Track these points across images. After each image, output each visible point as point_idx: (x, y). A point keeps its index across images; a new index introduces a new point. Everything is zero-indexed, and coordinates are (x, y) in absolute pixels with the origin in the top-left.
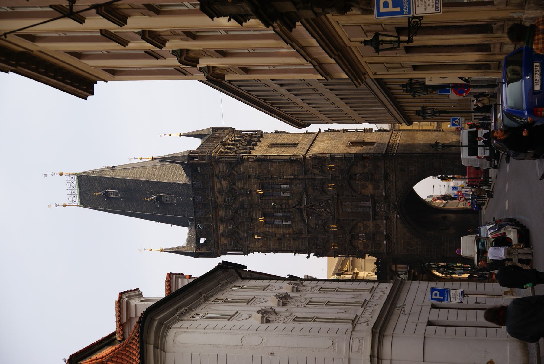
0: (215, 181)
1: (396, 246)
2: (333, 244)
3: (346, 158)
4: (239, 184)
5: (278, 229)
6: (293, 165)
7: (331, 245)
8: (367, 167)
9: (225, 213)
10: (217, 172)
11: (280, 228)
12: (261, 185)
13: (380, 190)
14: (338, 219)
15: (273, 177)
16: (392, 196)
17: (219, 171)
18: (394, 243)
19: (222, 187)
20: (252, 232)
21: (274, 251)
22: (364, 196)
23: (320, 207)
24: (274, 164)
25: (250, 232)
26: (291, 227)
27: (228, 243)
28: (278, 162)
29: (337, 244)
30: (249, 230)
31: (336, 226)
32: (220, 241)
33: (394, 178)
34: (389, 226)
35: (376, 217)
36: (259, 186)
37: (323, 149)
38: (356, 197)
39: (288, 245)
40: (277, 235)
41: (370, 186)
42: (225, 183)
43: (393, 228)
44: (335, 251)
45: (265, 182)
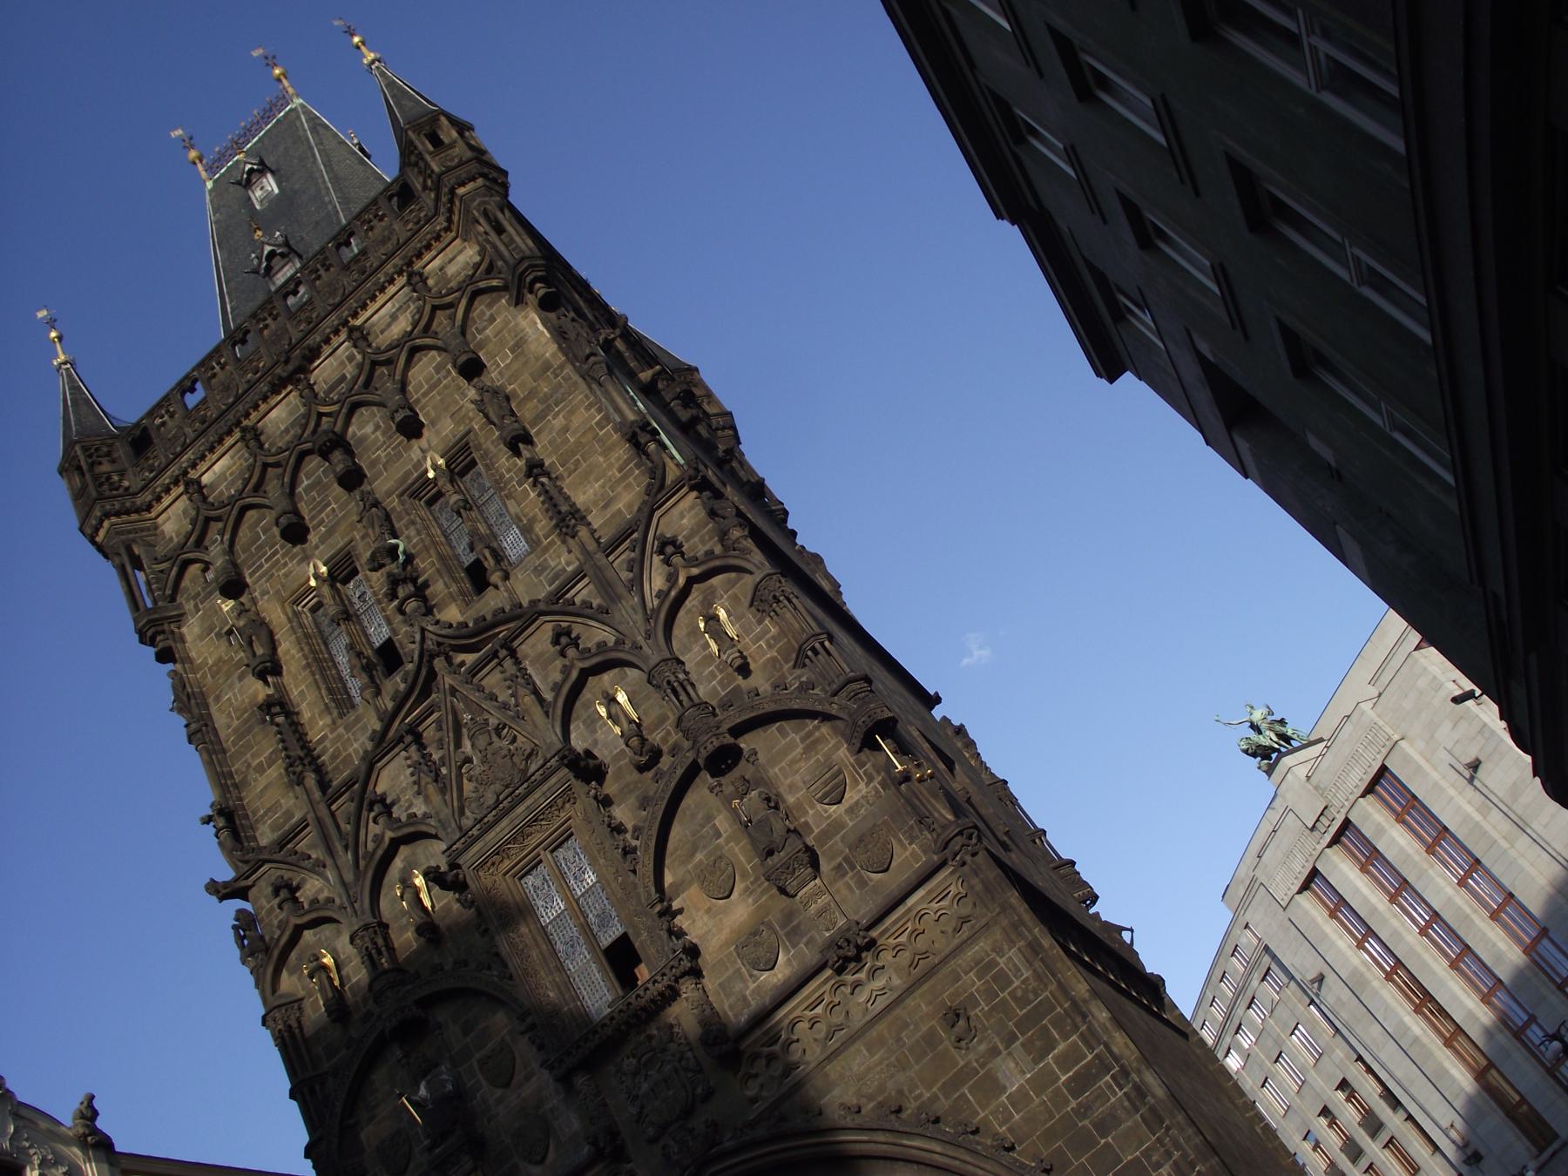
0: (392, 290)
2: (328, 960)
3: (813, 649)
4: (425, 369)
5: (305, 668)
6: (631, 479)
7: (317, 959)
9: (283, 428)
10: (437, 263)
11: (313, 674)
13: (752, 986)
15: (521, 445)
16: (762, 1086)
17: (441, 269)
19: (382, 332)
20: (248, 580)
21: (193, 726)
22: (661, 914)
23: (482, 748)
25: (247, 574)
26: (335, 713)
27: (171, 539)
29: (337, 983)
30: (254, 564)
31: (427, 903)
32: (166, 501)
33: (882, 1003)
35: (580, 1081)
36: (454, 440)
38: (634, 872)
39: (249, 765)
40: (270, 679)
41: (740, 910)
42: (403, 325)
44: (302, 999)
45: (484, 447)
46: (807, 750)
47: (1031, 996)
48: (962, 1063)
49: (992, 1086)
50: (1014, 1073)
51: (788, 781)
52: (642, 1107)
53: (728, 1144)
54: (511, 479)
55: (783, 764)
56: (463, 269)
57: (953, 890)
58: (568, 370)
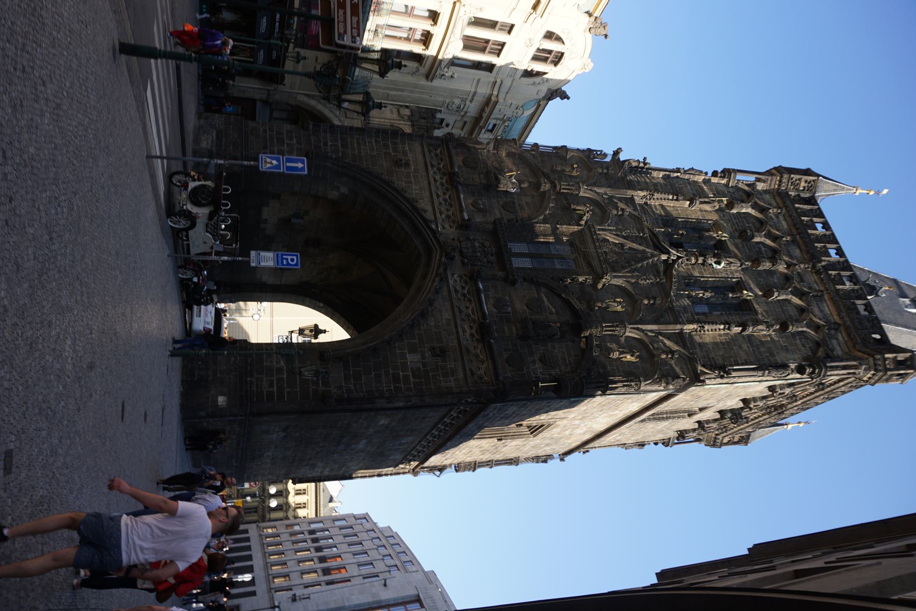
1: (428, 161)
3: (602, 382)
6: (707, 360)
8: (541, 361)
9: (791, 251)
12: (751, 311)
13: (491, 296)
14: (581, 225)
17: (837, 339)
18: (432, 166)
24: (745, 360)
28: (738, 365)
32: (778, 199)
34: (451, 205)
35: (490, 227)
37: (616, 409)
38: (552, 279)
43: (441, 199)
46: (565, 360)
47: (434, 381)
48: (426, 345)
49: (413, 350)
50: (412, 359)
51: (557, 346)
52: (471, 241)
53: (443, 259)
54: (729, 318)
55: (564, 350)
56: (833, 346)
57: (486, 378)
58: (766, 361)
